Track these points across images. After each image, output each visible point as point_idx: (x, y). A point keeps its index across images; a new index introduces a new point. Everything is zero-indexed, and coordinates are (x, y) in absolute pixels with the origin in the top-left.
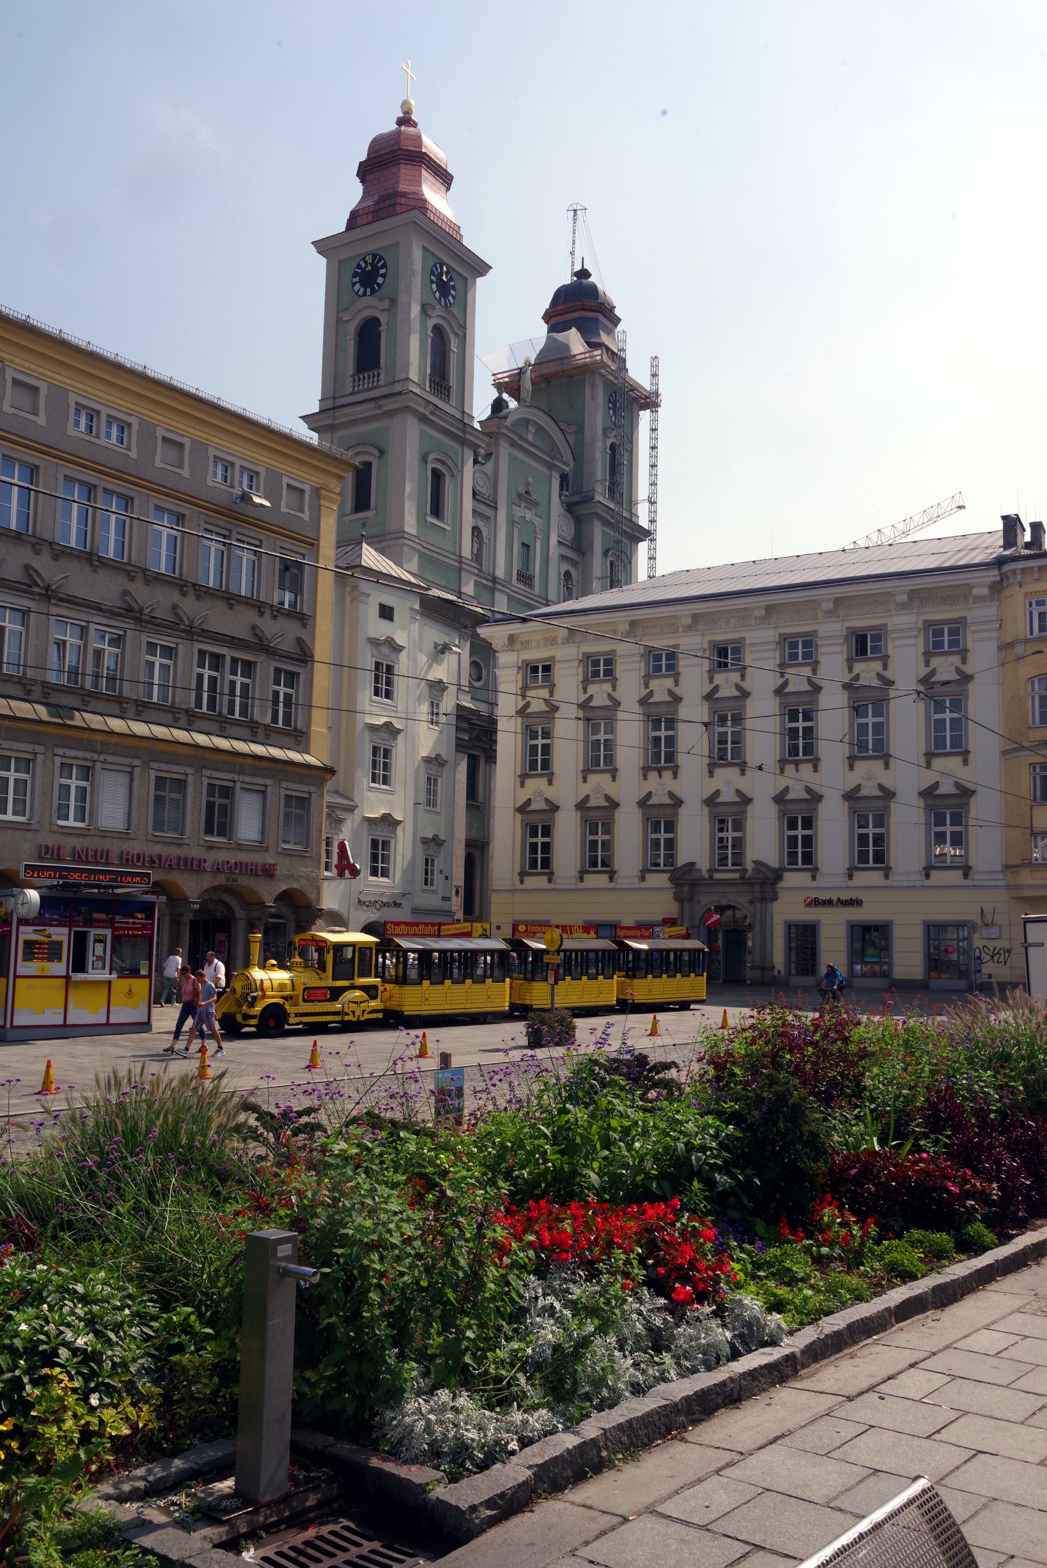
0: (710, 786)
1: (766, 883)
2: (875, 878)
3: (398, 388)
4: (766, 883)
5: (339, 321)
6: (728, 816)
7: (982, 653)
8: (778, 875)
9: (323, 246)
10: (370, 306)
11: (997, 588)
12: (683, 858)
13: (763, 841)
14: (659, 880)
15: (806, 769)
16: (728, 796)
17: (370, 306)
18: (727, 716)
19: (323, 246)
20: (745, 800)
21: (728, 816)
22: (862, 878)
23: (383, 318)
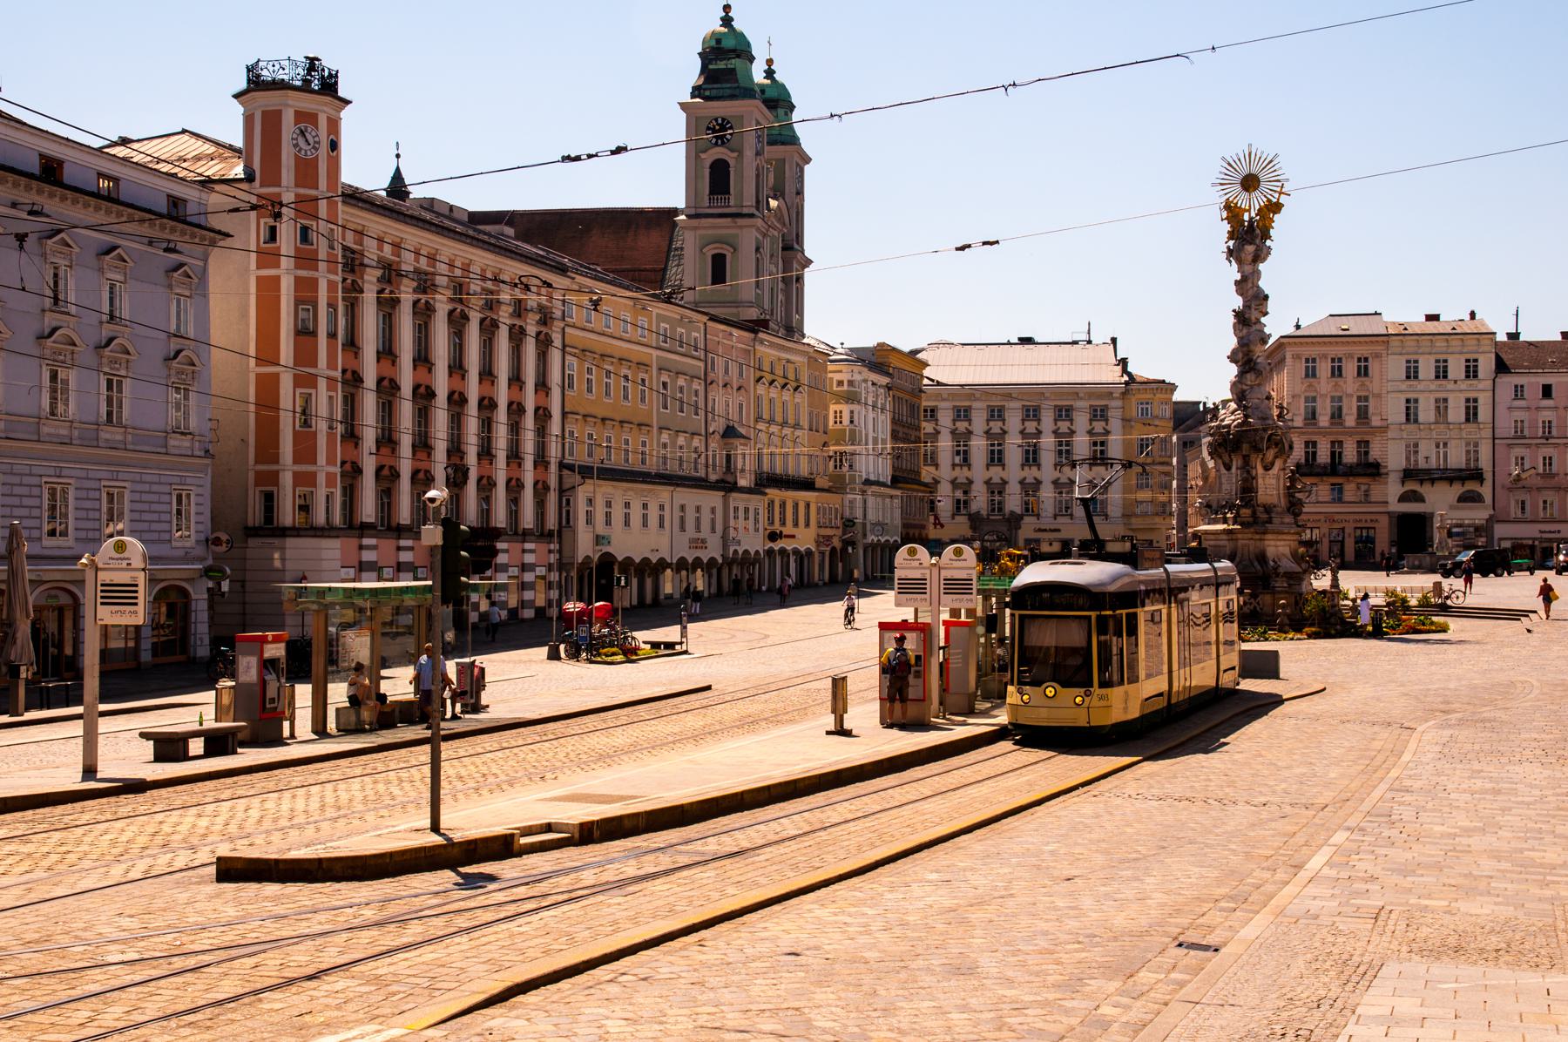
0: (987, 475)
1: (1014, 521)
2: (1066, 520)
3: (745, 211)
4: (1014, 521)
5: (697, 156)
6: (997, 489)
7: (1115, 424)
8: (1021, 517)
9: (683, 106)
10: (718, 153)
11: (1124, 394)
12: (974, 507)
13: (1013, 503)
14: (962, 519)
15: (1034, 469)
16: (996, 480)
17: (718, 153)
18: (996, 441)
19: (683, 106)
20: (1005, 482)
21: (997, 489)
22: (1060, 520)
23: (732, 163)
